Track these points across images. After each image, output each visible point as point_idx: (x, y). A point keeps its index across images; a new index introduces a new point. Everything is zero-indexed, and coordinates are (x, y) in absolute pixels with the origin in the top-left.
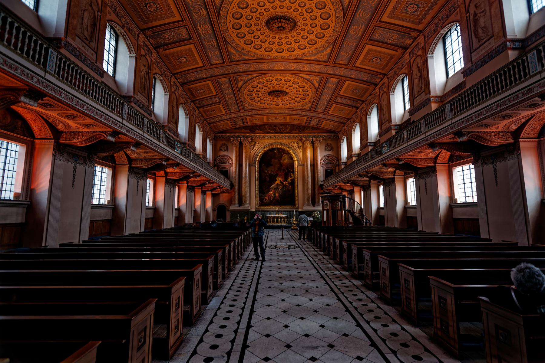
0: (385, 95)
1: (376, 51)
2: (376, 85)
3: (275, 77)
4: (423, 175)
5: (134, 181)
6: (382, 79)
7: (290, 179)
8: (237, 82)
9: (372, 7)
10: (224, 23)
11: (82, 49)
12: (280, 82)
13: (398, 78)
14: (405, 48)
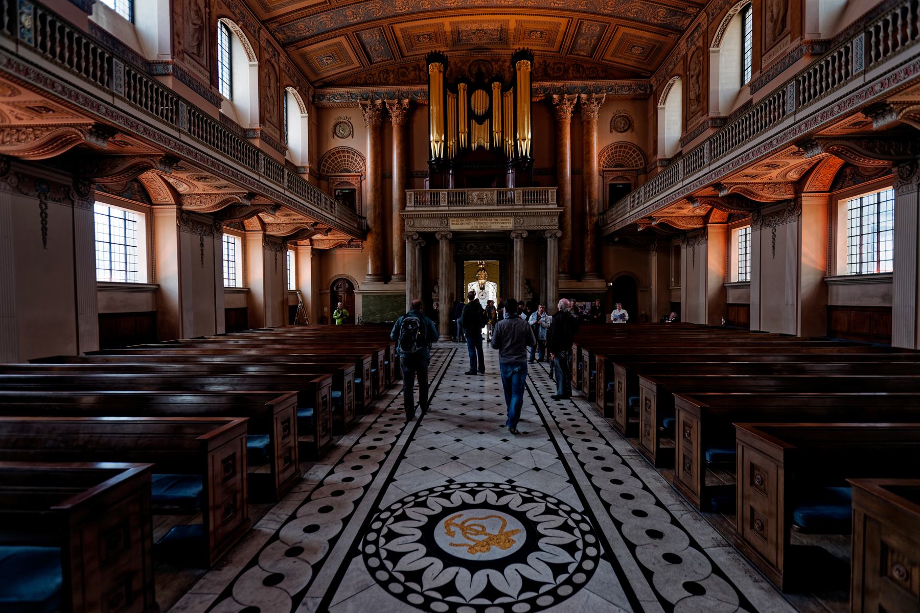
4: (771, 219)
5: (193, 238)
6: (696, 17)
13: (730, 12)
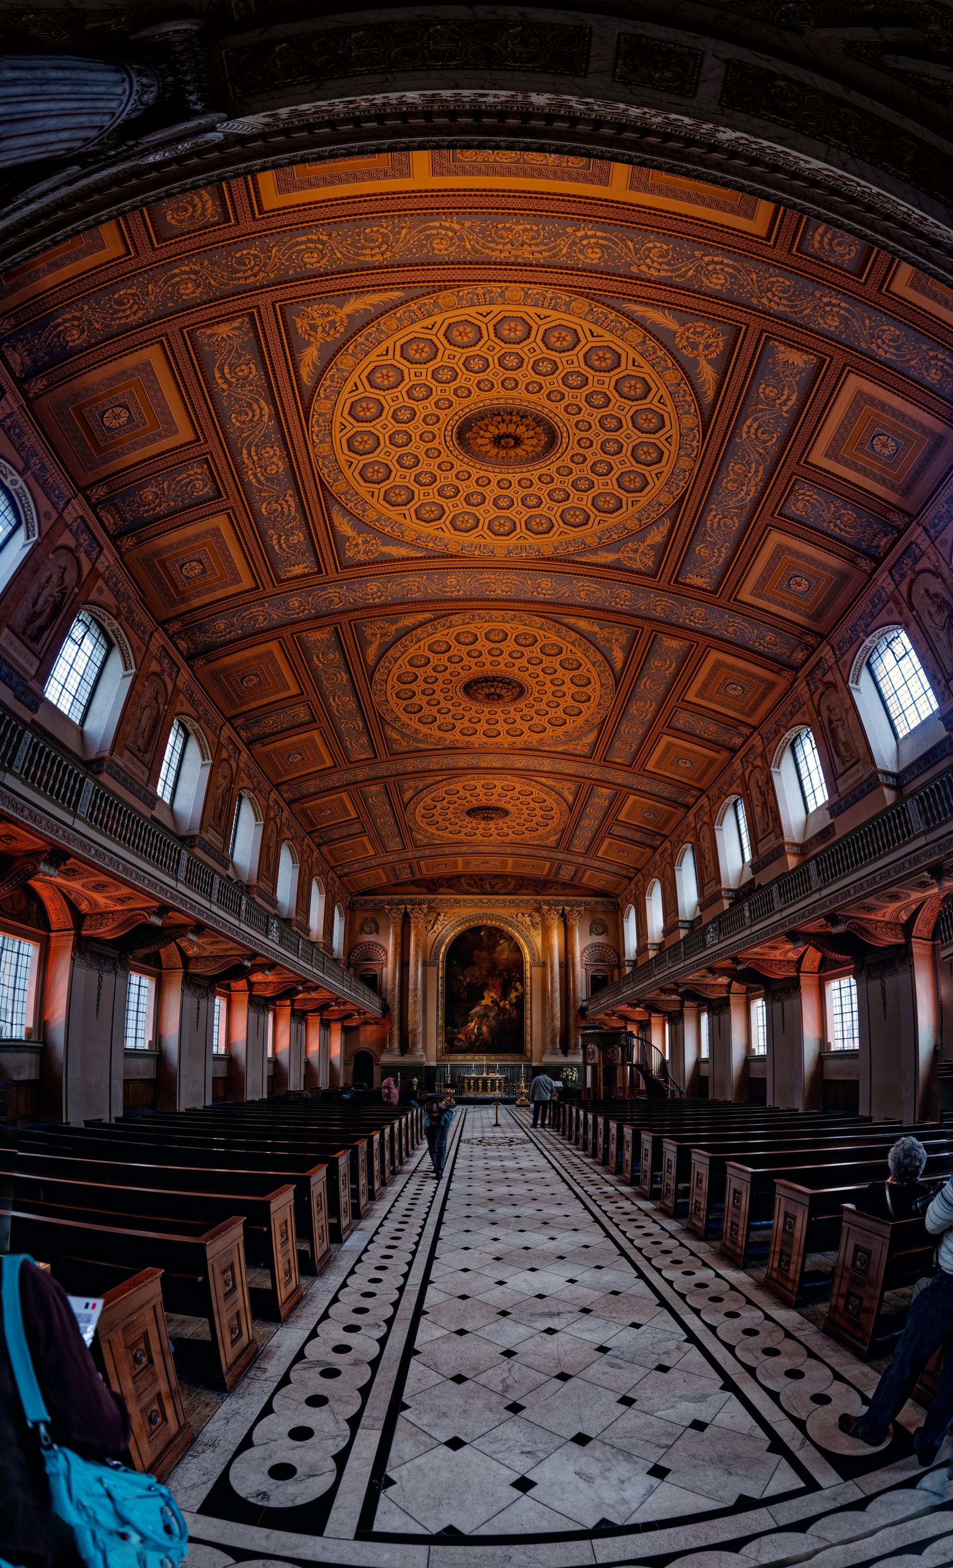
0: (705, 828)
1: (682, 748)
2: (688, 808)
3: (483, 782)
7: (513, 995)
8: (401, 791)
9: (665, 677)
10: (381, 690)
11: (131, 766)
12: (494, 791)
14: (734, 751)
